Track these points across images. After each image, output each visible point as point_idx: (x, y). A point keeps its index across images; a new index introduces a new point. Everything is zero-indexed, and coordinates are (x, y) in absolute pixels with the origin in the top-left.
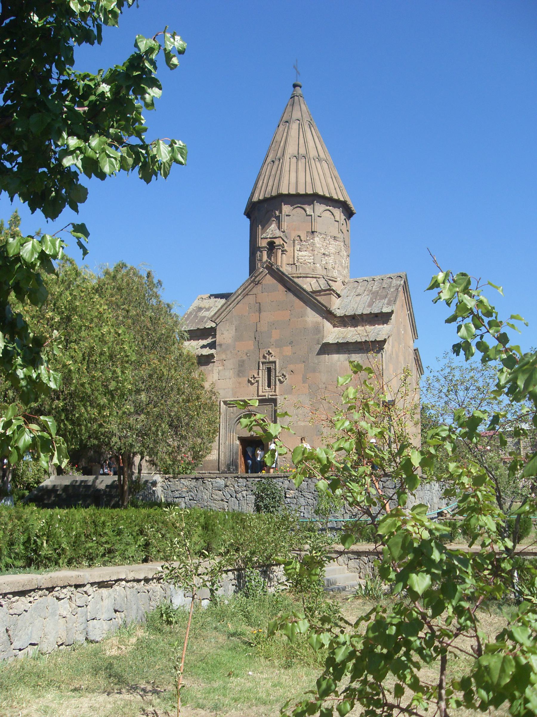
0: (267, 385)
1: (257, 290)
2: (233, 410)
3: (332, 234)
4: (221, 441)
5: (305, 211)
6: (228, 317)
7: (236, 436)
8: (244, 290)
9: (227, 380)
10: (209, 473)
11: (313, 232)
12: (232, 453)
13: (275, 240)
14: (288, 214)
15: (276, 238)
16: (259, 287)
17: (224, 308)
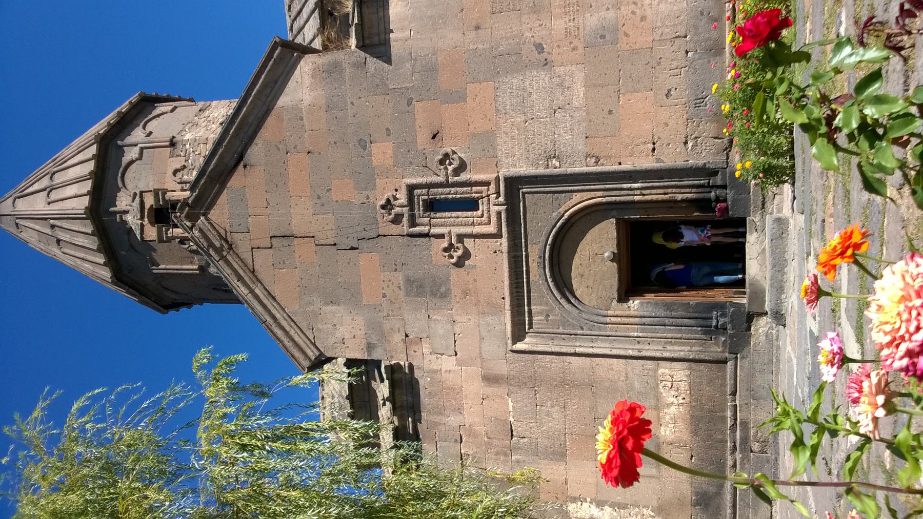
0: (470, 213)
1: (243, 245)
2: (540, 313)
3: (191, 115)
4: (630, 353)
5: (132, 162)
6: (304, 326)
7: (617, 308)
8: (240, 278)
9: (457, 329)
10: (734, 393)
11: (173, 144)
12: (667, 321)
13: (147, 206)
14: (131, 198)
15: (142, 204)
16: (237, 238)
17: (279, 333)
